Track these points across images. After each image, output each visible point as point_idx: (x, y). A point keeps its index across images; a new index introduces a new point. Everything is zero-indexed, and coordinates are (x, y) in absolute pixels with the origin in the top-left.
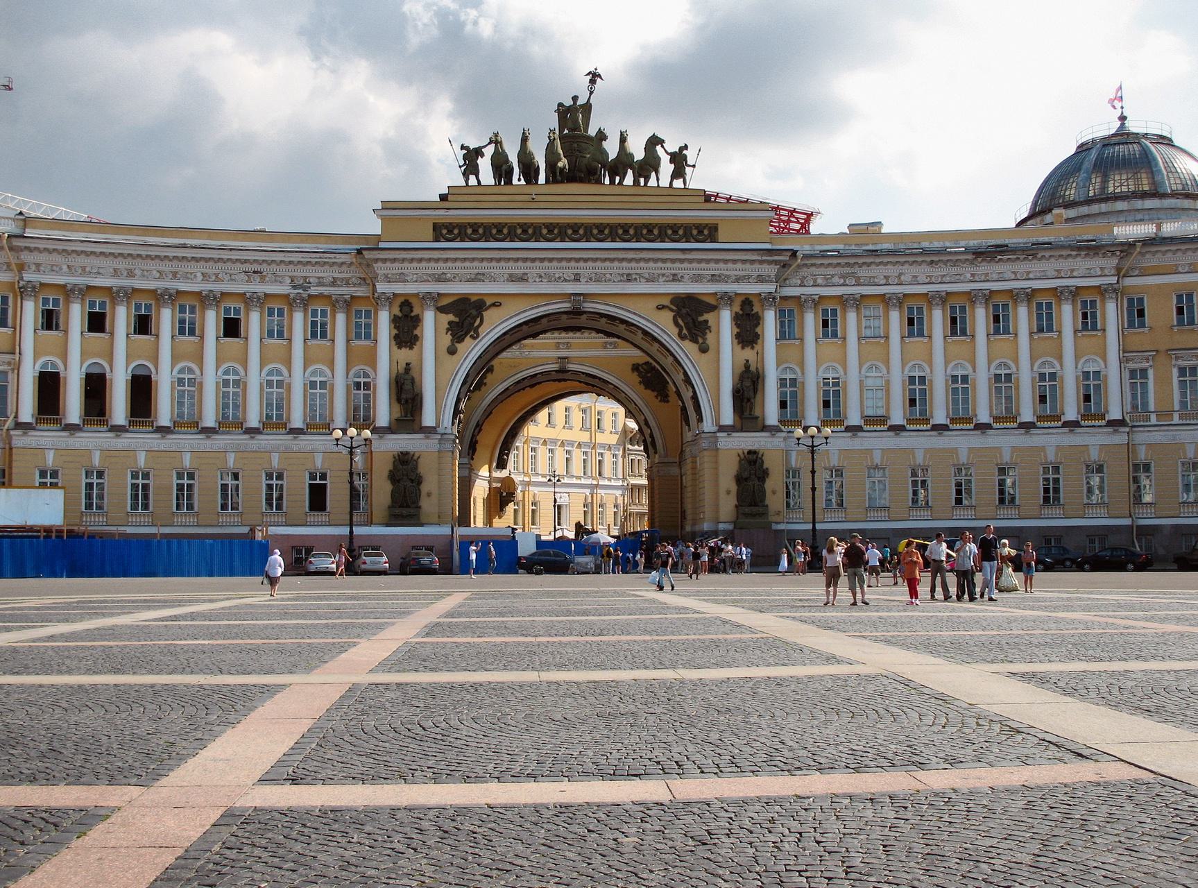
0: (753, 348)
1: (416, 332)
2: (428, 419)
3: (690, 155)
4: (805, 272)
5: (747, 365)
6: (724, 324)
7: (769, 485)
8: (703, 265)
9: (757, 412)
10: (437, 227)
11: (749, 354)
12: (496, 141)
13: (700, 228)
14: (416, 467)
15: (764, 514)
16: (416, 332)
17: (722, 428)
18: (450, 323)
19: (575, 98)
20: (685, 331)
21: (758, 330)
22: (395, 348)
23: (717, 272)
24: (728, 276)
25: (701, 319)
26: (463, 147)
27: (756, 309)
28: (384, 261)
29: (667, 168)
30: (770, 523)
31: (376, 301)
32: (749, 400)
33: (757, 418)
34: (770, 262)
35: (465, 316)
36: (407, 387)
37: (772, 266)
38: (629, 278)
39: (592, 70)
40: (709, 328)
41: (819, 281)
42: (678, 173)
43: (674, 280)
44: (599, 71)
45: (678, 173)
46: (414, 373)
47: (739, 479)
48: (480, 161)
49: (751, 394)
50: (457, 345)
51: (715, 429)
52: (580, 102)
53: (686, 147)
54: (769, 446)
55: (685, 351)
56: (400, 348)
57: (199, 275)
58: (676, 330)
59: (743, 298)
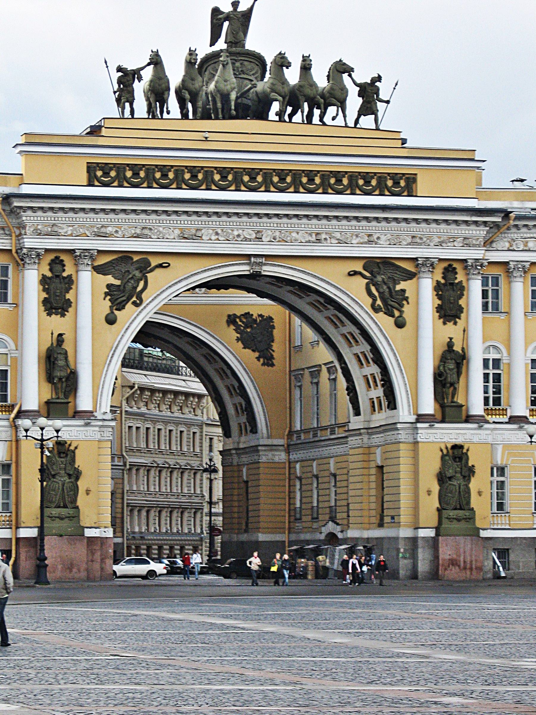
0: (455, 323)
1: (68, 296)
2: (84, 402)
4: (514, 234)
5: (450, 344)
6: (424, 293)
7: (474, 485)
9: (460, 399)
10: (91, 168)
11: (451, 330)
13: (396, 178)
14: (73, 460)
15: (471, 519)
16: (68, 296)
17: (421, 418)
18: (109, 286)
19: (235, 5)
20: (379, 302)
21: (462, 302)
22: (45, 314)
25: (398, 288)
26: (119, 69)
27: (460, 277)
29: (354, 102)
30: (478, 529)
31: (21, 258)
32: (452, 384)
33: (462, 406)
35: (127, 276)
36: (61, 363)
37: (482, 228)
40: (406, 299)
41: (531, 245)
42: (368, 108)
43: (370, 242)
46: (67, 346)
47: (441, 478)
49: (455, 376)
50: (116, 312)
51: (413, 419)
52: (242, 8)
53: (379, 79)
54: (476, 439)
55: (379, 325)
58: (370, 301)
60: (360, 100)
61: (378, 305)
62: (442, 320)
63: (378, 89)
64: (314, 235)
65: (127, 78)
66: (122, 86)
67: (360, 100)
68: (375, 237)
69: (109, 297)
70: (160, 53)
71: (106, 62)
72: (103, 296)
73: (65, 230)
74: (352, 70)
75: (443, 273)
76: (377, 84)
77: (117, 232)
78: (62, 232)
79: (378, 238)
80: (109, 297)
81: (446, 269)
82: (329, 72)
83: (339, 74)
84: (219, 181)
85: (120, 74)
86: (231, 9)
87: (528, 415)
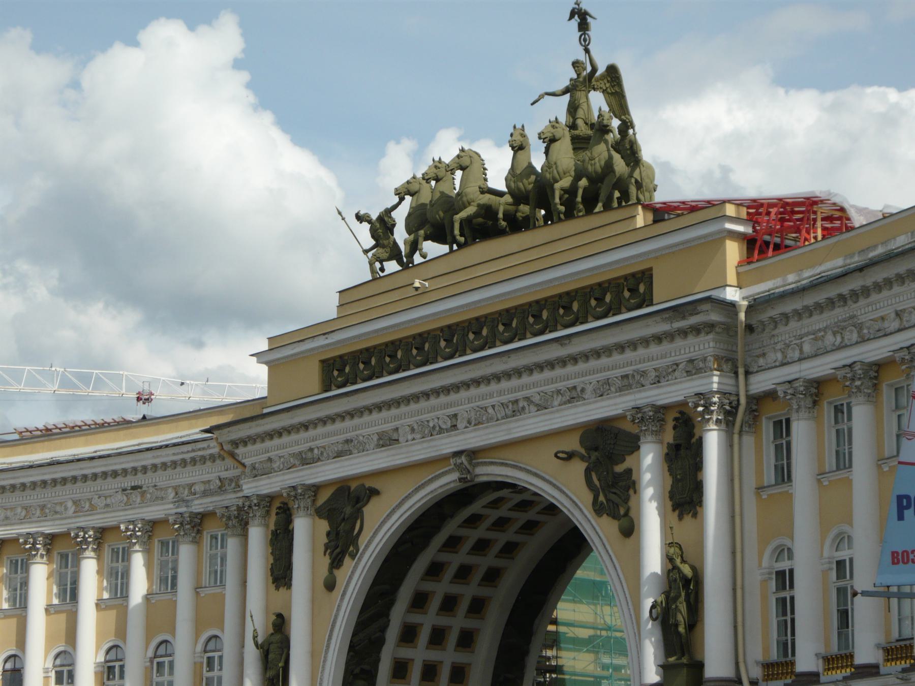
0: (695, 515)
8: (604, 361)
18: (328, 534)
20: (602, 498)
22: (272, 587)
23: (628, 370)
24: (643, 374)
25: (619, 469)
26: (360, 218)
27: (697, 431)
28: (245, 442)
34: (696, 330)
37: (703, 338)
38: (515, 410)
43: (572, 400)
44: (584, 6)
50: (336, 572)
56: (277, 588)
57: (70, 504)
59: (674, 414)
61: (602, 503)
62: (677, 512)
64: (510, 406)
68: (579, 389)
69: (329, 551)
71: (340, 213)
72: (322, 549)
73: (278, 464)
75: (675, 428)
77: (322, 453)
78: (275, 465)
79: (583, 390)
80: (329, 551)
81: (676, 419)
87: (821, 670)
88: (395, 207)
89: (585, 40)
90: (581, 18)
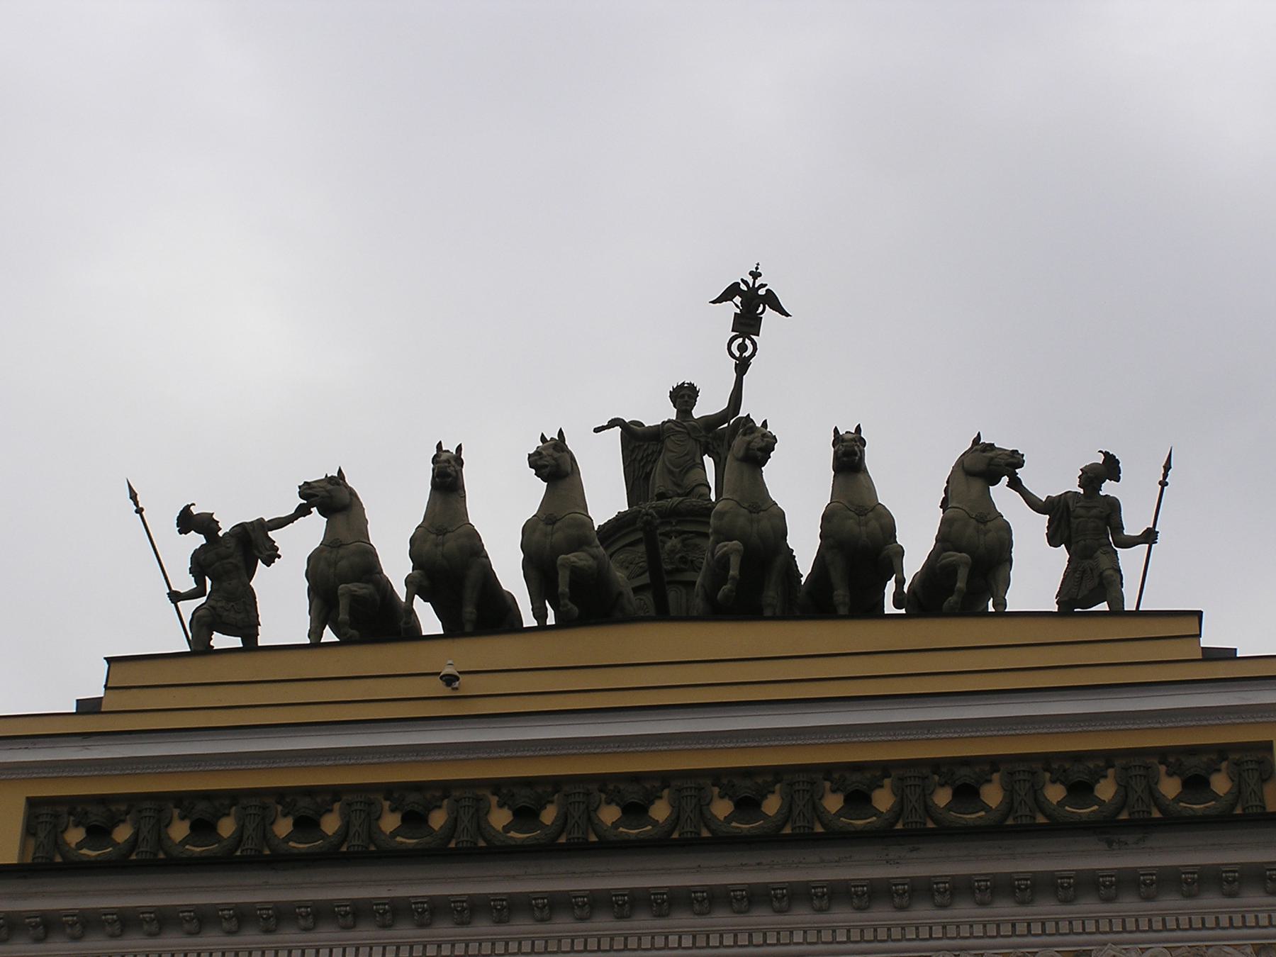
3: (1133, 500)
12: (331, 498)
19: (684, 396)
26: (187, 521)
39: (739, 274)
44: (771, 281)
45: (1090, 582)
48: (264, 580)
52: (704, 408)
53: (1110, 467)
60: (1061, 556)
63: (1113, 506)
65: (229, 558)
66: (209, 582)
67: (1061, 556)
70: (349, 481)
71: (133, 496)
74: (1015, 460)
76: (1108, 488)
82: (946, 491)
83: (977, 484)
84: (507, 829)
85: (196, 540)
86: (671, 413)
88: (280, 523)
89: (742, 348)
90: (751, 305)
